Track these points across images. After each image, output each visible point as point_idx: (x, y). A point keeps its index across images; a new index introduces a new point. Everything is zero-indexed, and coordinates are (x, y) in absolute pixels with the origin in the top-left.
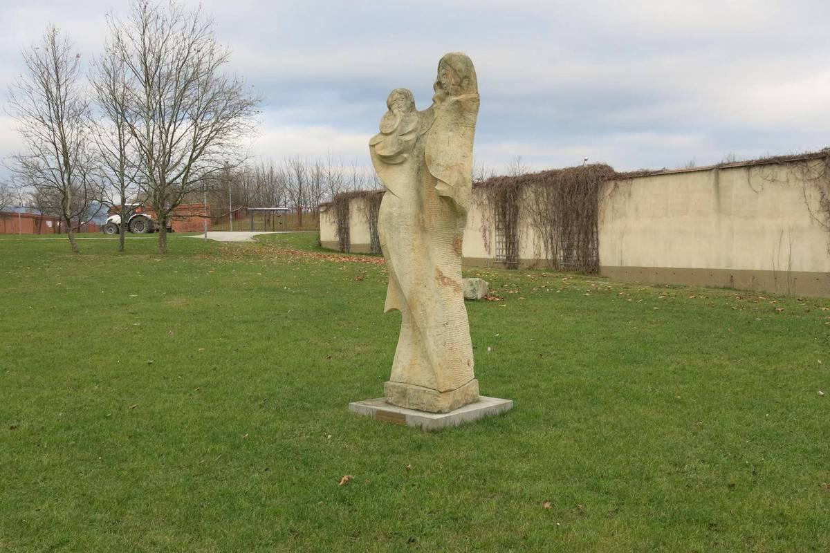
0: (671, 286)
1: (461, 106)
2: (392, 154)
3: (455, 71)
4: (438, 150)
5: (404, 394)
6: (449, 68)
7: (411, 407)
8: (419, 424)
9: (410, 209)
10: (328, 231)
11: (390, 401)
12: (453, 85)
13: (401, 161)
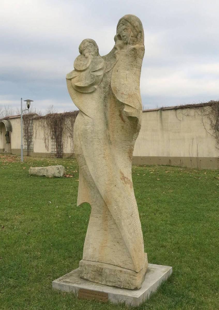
0: (148, 165)
1: (136, 53)
2: (86, 85)
3: (134, 27)
4: (120, 84)
5: (100, 272)
6: (129, 24)
7: (108, 284)
8: (122, 302)
9: (100, 127)
10: (17, 141)
11: (85, 277)
12: (132, 36)
13: (92, 91)
